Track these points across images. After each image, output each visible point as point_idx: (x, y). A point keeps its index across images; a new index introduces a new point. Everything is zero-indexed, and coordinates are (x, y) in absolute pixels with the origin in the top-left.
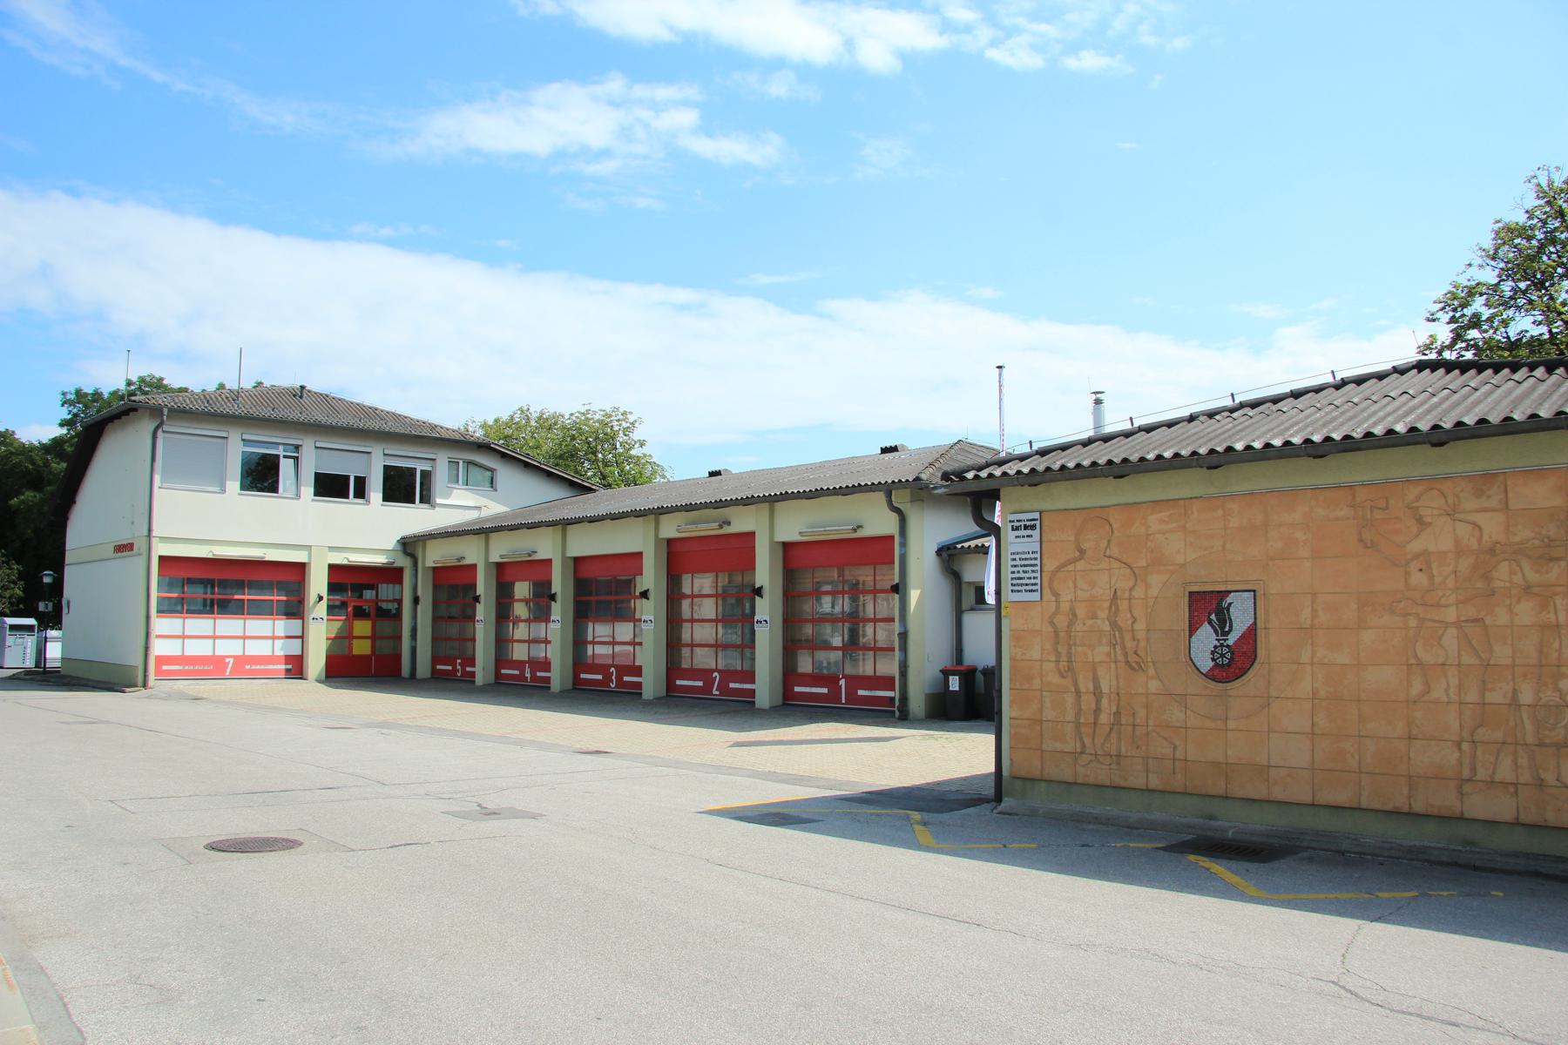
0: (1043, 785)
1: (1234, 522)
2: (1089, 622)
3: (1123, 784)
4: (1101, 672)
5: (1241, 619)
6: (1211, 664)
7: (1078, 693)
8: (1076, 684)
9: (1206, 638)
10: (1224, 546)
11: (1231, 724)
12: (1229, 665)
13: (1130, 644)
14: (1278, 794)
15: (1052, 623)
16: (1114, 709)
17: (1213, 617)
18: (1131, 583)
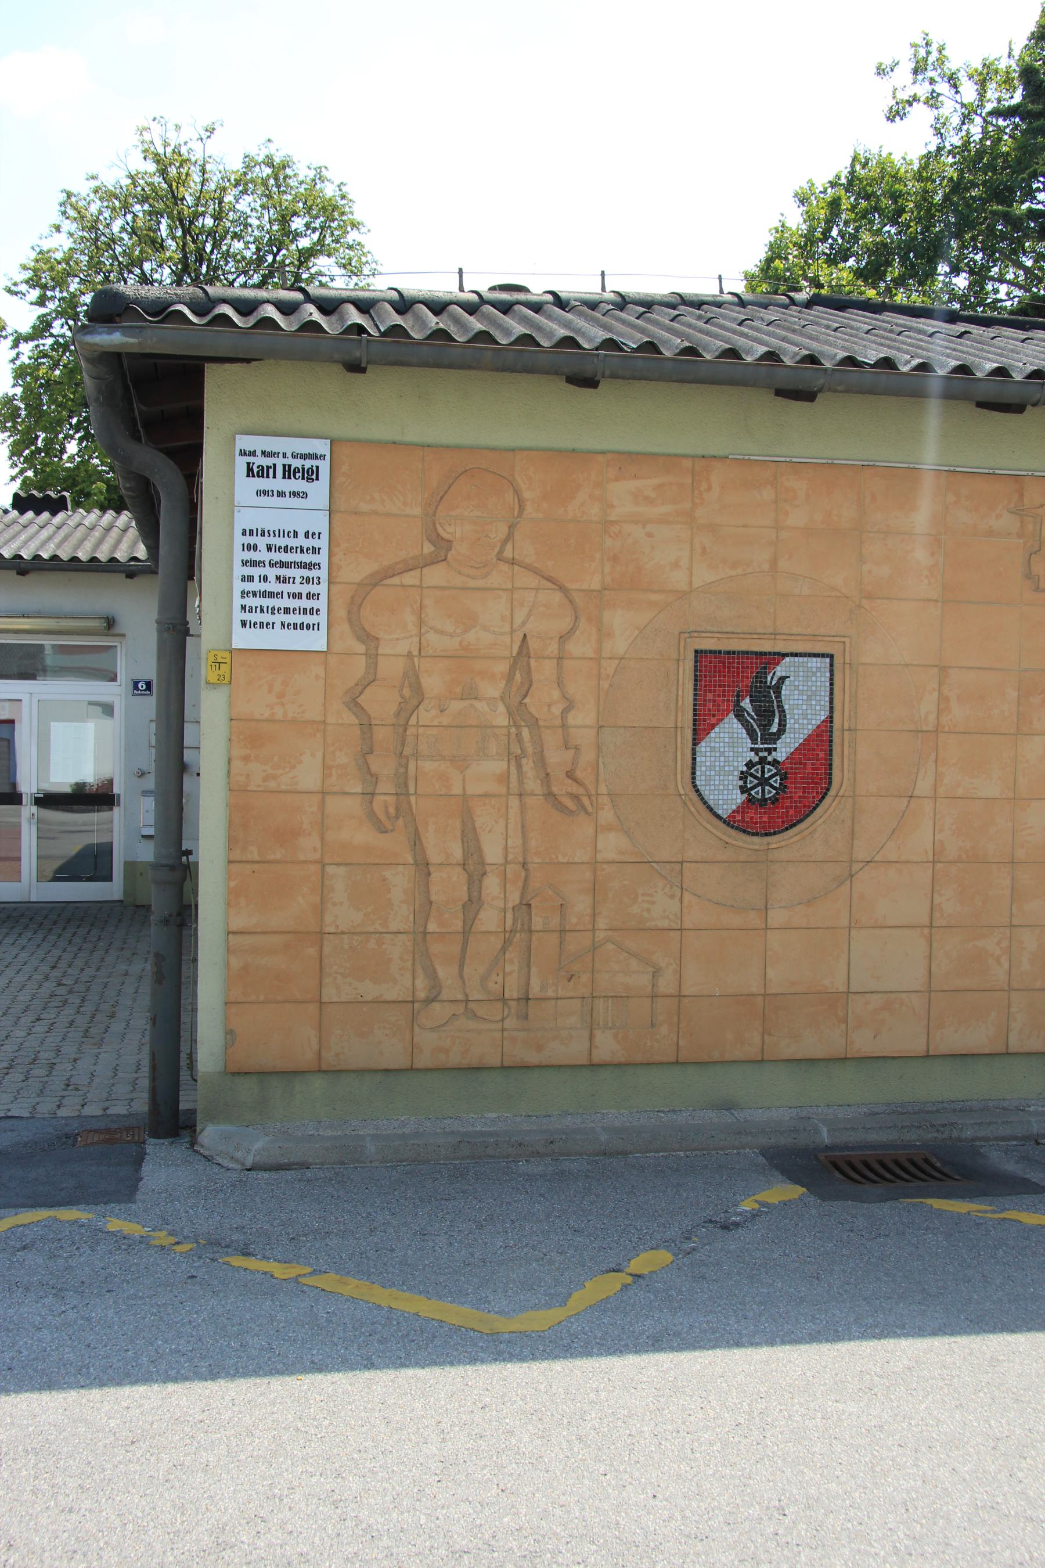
0: (318, 1083)
1: (797, 518)
2: (456, 706)
3: (533, 1057)
4: (484, 818)
5: (802, 709)
6: (739, 798)
7: (423, 867)
8: (416, 842)
9: (729, 746)
10: (774, 562)
11: (777, 916)
12: (775, 800)
13: (557, 758)
14: (864, 1043)
15: (354, 704)
16: (514, 898)
17: (746, 703)
18: (564, 624)
